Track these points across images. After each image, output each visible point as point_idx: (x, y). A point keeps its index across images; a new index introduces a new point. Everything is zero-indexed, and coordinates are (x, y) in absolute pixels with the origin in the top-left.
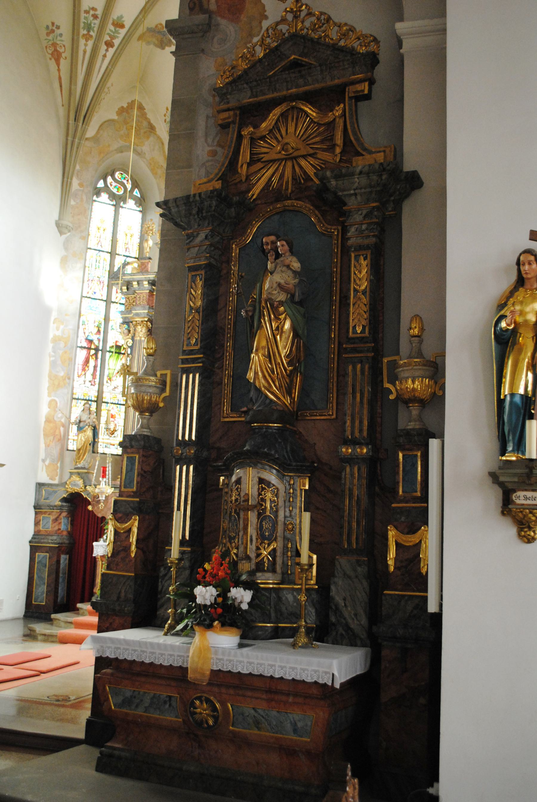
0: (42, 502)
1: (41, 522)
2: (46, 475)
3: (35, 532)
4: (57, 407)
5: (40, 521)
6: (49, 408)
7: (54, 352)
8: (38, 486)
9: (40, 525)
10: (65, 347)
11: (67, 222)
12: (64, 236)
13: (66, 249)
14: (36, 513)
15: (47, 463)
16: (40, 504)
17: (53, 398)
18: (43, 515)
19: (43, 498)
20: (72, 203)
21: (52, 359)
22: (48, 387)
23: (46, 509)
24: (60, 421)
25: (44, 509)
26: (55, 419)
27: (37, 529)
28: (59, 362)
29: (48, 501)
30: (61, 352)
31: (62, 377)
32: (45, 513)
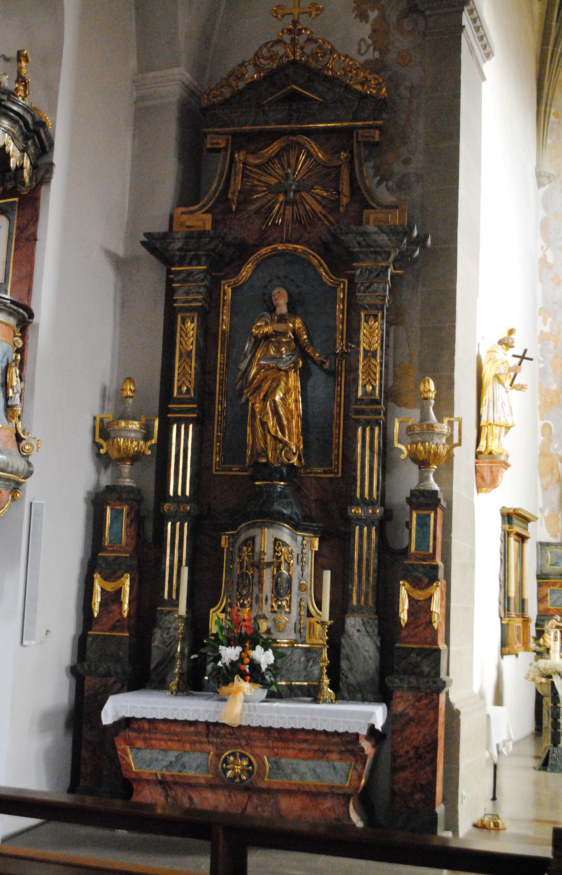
0: (548, 569)
1: (549, 598)
2: (546, 530)
3: (539, 611)
4: (551, 434)
5: (547, 595)
6: (543, 435)
7: (543, 356)
8: (539, 546)
9: (547, 601)
10: (555, 348)
11: (548, 169)
12: (543, 189)
13: (546, 207)
14: (539, 585)
15: (546, 513)
16: (544, 572)
17: (546, 421)
18: (552, 588)
19: (549, 563)
20: (549, 141)
21: (542, 365)
22: (540, 406)
23: (555, 579)
24: (557, 454)
25: (553, 579)
26: (552, 451)
27: (542, 607)
28: (550, 371)
29: (557, 567)
30: (550, 356)
31: (555, 391)
32: (554, 584)
